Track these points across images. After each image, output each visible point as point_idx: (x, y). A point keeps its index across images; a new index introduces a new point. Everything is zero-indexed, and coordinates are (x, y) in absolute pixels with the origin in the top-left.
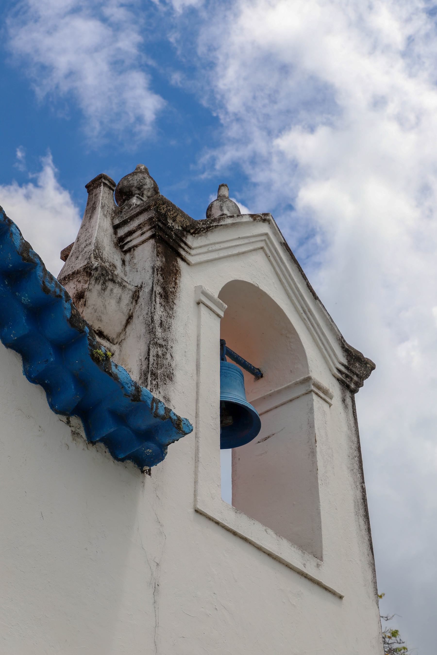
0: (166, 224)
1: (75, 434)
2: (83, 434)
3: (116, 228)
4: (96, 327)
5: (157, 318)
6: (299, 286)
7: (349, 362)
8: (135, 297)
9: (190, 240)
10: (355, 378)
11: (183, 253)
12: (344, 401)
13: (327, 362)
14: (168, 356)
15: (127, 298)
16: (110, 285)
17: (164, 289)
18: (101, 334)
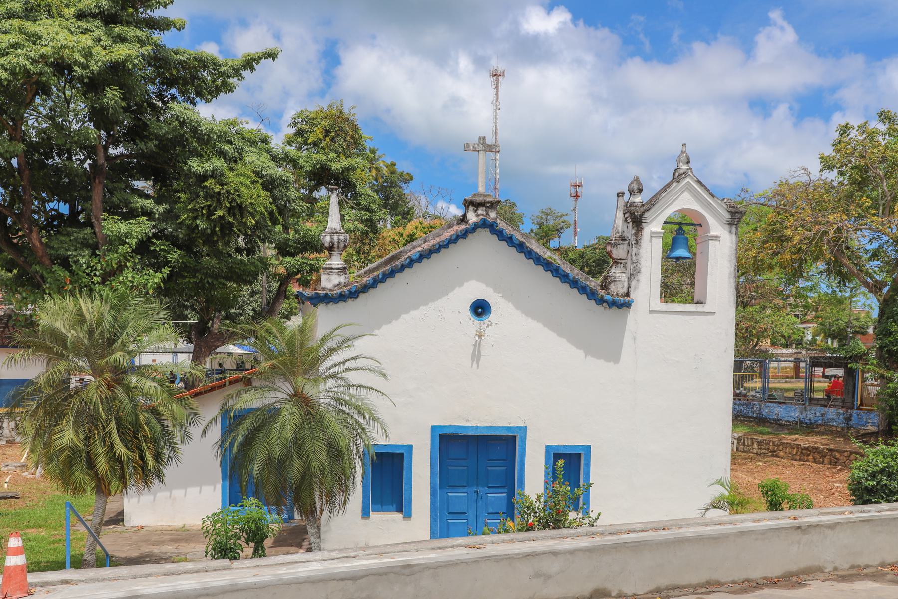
0: (635, 216)
1: (605, 308)
2: (607, 307)
3: (624, 214)
4: (618, 258)
5: (633, 254)
6: (705, 195)
7: (732, 216)
8: (629, 244)
9: (646, 215)
10: (737, 220)
11: (643, 221)
12: (730, 232)
13: (721, 220)
14: (639, 264)
15: (625, 246)
16: (618, 246)
17: (636, 240)
18: (621, 259)
